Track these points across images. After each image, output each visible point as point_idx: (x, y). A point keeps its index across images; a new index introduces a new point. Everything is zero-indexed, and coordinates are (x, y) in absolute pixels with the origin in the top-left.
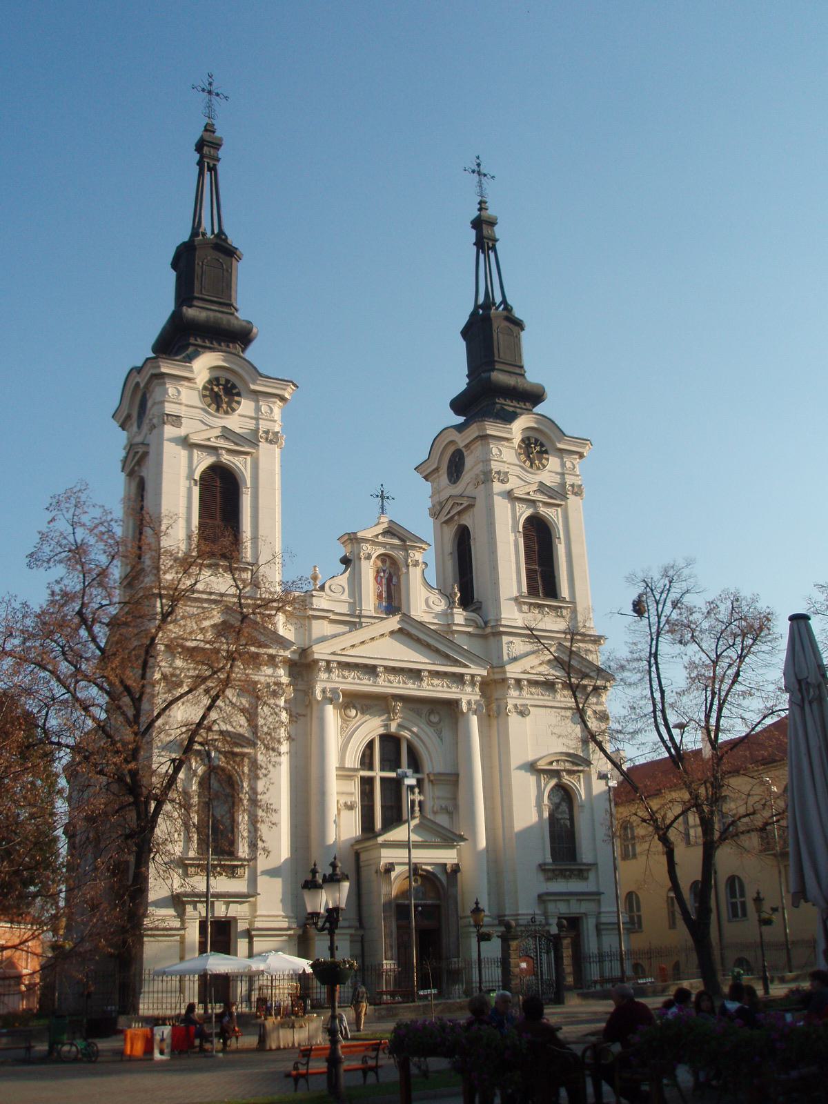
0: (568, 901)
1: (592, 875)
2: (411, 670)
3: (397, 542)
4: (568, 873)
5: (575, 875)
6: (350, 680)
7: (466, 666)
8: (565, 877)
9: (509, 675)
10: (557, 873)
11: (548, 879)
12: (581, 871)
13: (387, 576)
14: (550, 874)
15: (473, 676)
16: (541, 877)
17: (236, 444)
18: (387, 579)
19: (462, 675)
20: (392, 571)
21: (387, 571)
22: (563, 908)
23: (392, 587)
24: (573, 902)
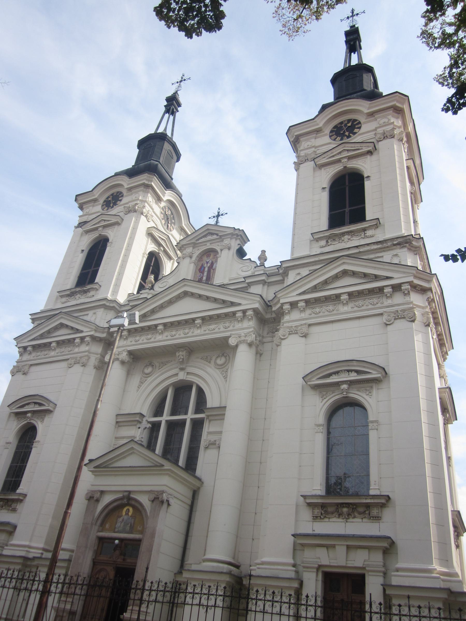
0: (333, 546)
1: (387, 514)
2: (187, 322)
3: (215, 237)
4: (345, 510)
5: (360, 513)
6: (140, 342)
7: (239, 304)
8: (340, 515)
9: (282, 301)
10: (330, 509)
11: (315, 518)
12: (368, 506)
13: (209, 265)
14: (317, 511)
15: (244, 312)
16: (306, 514)
17: (108, 221)
18: (209, 267)
19: (234, 313)
20: (214, 260)
21: (210, 262)
22: (324, 558)
23: (212, 271)
24: (341, 551)
